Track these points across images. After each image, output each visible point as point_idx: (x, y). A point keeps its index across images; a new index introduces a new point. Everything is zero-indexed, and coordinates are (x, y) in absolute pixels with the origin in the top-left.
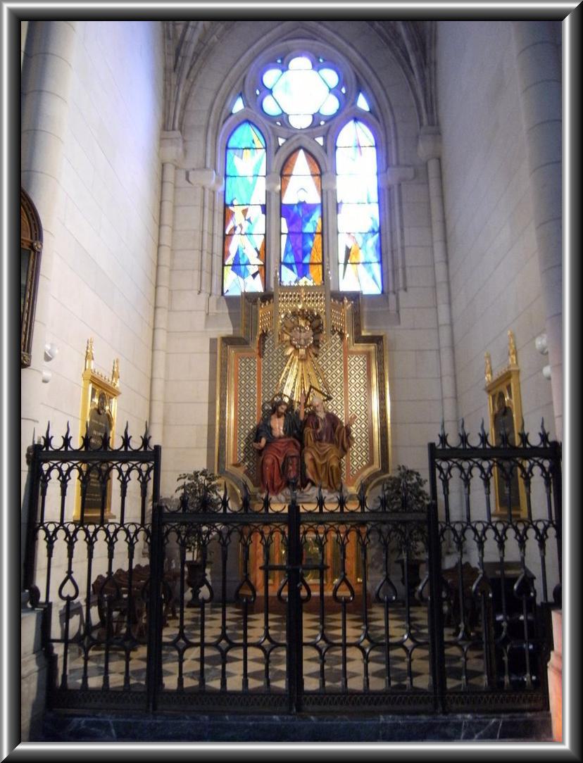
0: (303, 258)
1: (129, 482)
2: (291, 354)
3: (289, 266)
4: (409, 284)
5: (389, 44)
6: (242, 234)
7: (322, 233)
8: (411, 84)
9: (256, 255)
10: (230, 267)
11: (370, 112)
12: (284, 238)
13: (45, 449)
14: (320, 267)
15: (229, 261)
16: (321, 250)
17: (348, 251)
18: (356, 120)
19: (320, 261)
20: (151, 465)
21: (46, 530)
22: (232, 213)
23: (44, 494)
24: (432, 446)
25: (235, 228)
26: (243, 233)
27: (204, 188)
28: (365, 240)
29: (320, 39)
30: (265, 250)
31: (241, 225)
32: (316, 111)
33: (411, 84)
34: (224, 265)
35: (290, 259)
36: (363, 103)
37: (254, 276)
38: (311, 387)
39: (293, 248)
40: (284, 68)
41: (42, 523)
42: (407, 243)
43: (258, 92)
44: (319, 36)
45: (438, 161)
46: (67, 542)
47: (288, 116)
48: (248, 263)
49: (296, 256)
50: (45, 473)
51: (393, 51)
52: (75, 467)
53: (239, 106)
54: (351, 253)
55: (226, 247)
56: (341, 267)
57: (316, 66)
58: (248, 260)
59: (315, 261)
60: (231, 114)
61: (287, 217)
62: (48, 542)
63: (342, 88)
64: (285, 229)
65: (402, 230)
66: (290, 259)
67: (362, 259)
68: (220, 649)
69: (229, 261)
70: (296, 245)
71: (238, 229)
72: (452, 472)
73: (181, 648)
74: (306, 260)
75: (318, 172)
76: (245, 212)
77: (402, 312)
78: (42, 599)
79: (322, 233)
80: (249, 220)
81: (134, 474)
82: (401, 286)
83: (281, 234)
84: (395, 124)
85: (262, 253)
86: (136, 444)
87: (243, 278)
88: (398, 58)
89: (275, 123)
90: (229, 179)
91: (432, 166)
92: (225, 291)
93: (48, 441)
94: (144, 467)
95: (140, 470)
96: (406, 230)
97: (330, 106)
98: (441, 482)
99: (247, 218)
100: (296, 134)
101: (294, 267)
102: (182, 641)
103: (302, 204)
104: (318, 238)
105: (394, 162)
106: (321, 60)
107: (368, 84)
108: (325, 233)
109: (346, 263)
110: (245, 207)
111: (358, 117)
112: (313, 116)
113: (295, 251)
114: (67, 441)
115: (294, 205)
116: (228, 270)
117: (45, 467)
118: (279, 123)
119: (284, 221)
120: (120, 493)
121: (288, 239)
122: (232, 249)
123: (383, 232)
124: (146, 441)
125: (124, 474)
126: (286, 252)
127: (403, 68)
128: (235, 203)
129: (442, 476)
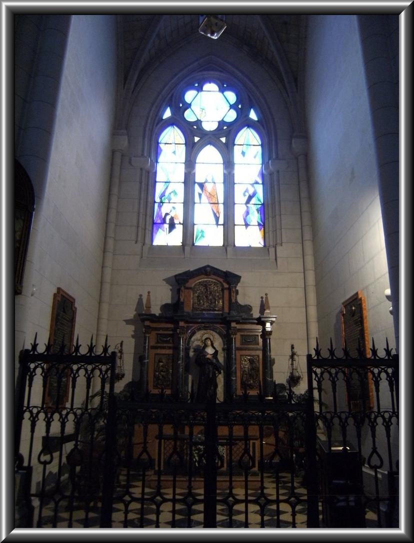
1: (329, 378)
13: (32, 353)
18: (249, 126)
20: (108, 367)
21: (31, 412)
23: (30, 386)
24: (309, 357)
27: (141, 169)
32: (220, 119)
36: (253, 115)
40: (200, 89)
41: (28, 407)
46: (60, 422)
50: (32, 370)
52: (83, 367)
53: (168, 114)
57: (222, 90)
60: (163, 119)
62: (31, 421)
68: (259, 504)
72: (353, 376)
73: (231, 503)
77: (278, 260)
78: (26, 464)
81: (97, 372)
86: (99, 351)
93: (35, 346)
94: (104, 368)
95: (101, 370)
97: (232, 116)
98: (316, 383)
102: (231, 499)
111: (250, 124)
112: (219, 122)
114: (91, 349)
117: (32, 366)
120: (85, 386)
124: (105, 349)
125: (104, 373)
129: (317, 379)
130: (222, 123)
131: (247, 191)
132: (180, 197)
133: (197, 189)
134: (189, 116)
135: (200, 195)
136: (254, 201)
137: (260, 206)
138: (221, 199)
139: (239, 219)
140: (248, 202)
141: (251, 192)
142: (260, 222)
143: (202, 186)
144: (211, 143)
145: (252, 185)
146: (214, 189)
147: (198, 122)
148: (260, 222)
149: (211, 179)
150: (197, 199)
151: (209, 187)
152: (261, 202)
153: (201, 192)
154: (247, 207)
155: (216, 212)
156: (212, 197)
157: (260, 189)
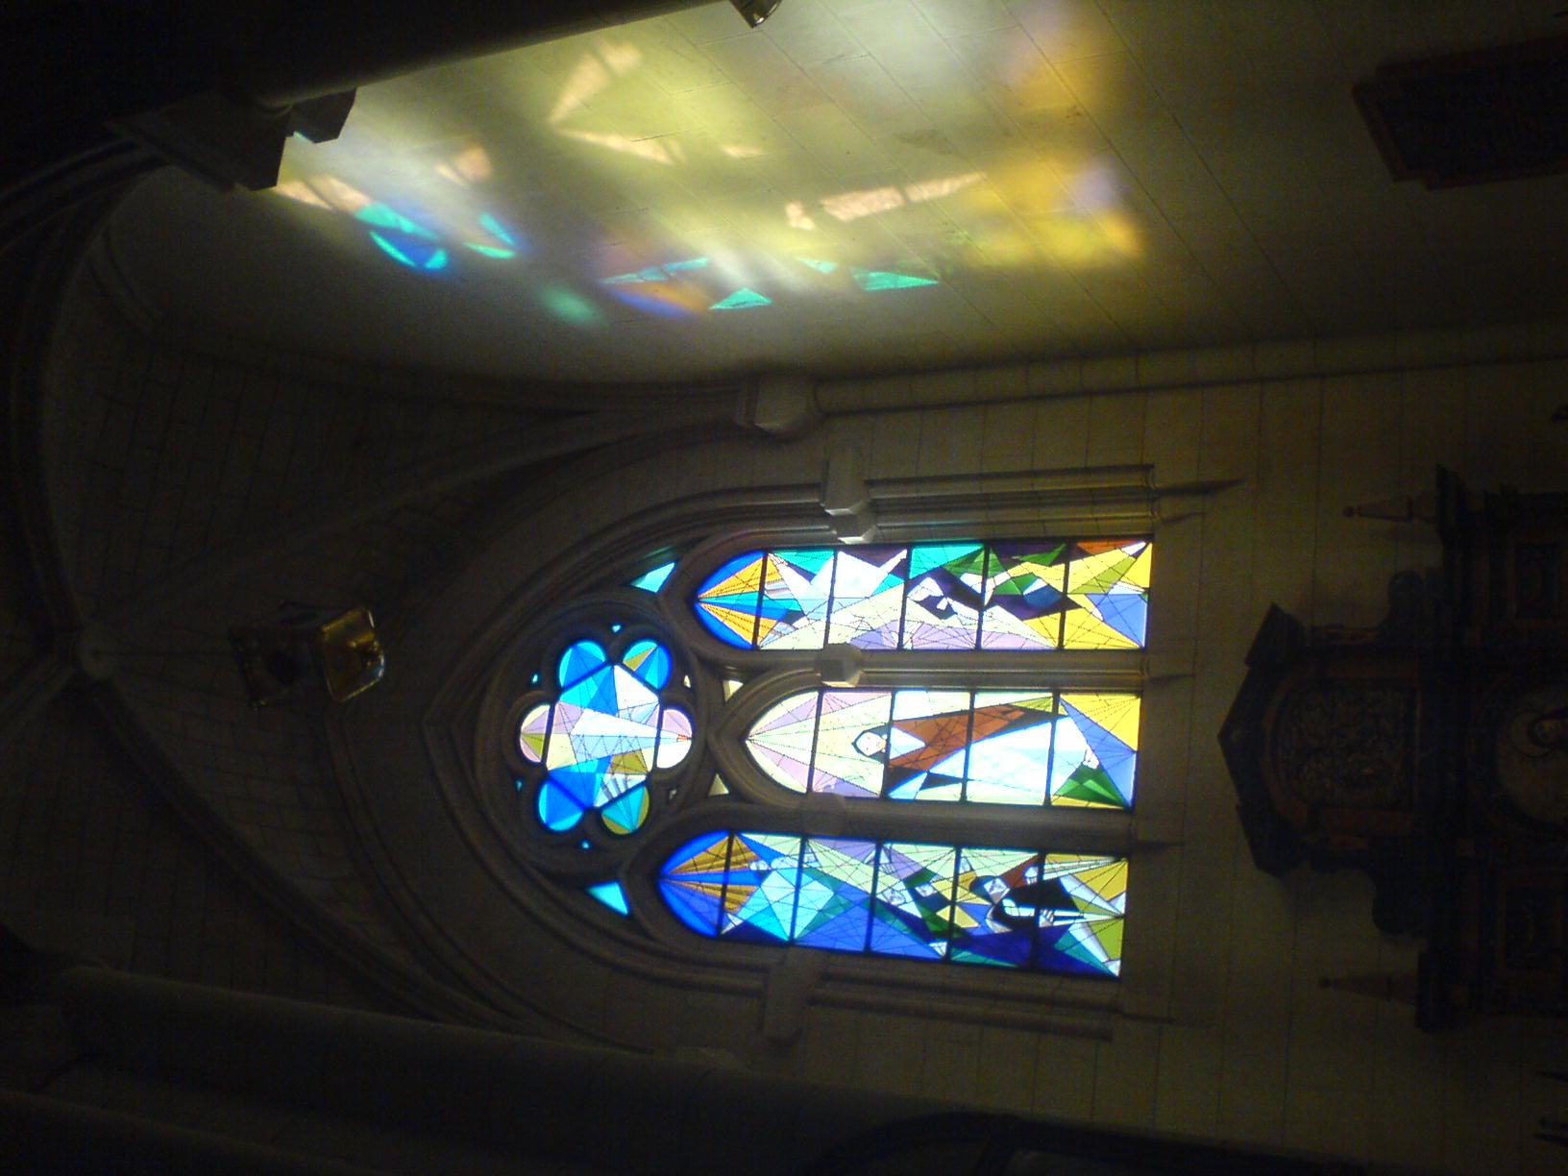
18: (692, 599)
27: (813, 1001)
53: (612, 896)
111: (687, 590)
112: (665, 703)
130: (669, 696)
131: (930, 604)
132: (936, 858)
133: (910, 790)
134: (627, 818)
135: (933, 781)
136: (971, 580)
137: (992, 556)
138: (956, 701)
139: (1037, 633)
140: (973, 599)
141: (931, 587)
142: (1054, 555)
143: (897, 772)
144: (744, 734)
145: (910, 585)
146: (912, 726)
147: (657, 782)
148: (1054, 555)
149: (875, 737)
150: (949, 793)
151: (904, 744)
152: (975, 554)
153: (922, 778)
154: (992, 603)
155: (1003, 723)
156: (945, 735)
157: (928, 557)
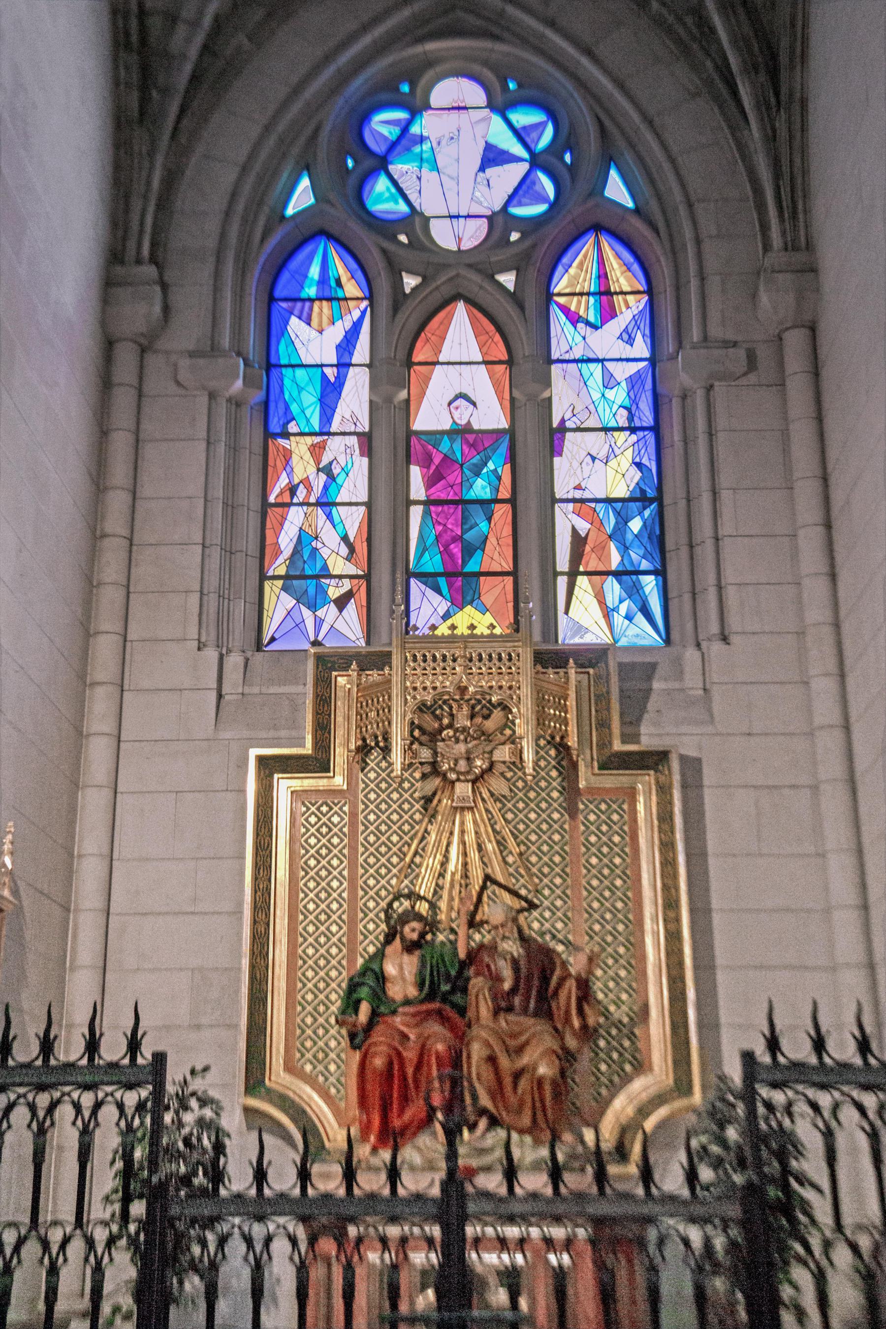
0: (465, 563)
2: (434, 794)
3: (427, 578)
4: (734, 622)
5: (686, 51)
6: (309, 504)
7: (512, 501)
8: (741, 147)
9: (344, 550)
10: (280, 583)
11: (637, 211)
12: (416, 514)
14: (509, 580)
15: (279, 567)
16: (510, 541)
17: (578, 542)
19: (508, 566)
22: (287, 456)
25: (292, 490)
26: (312, 500)
28: (623, 520)
29: (506, 35)
30: (369, 540)
31: (306, 482)
33: (741, 147)
34: (263, 577)
35: (433, 563)
37: (341, 603)
38: (487, 878)
39: (438, 537)
42: (726, 529)
43: (350, 163)
44: (508, 29)
45: (807, 332)
47: (426, 220)
48: (325, 573)
49: (446, 552)
51: (696, 67)
54: (588, 548)
55: (269, 533)
56: (562, 583)
58: (325, 567)
59: (496, 568)
60: (283, 217)
61: (426, 462)
63: (565, 152)
64: (418, 489)
65: (715, 493)
66: (433, 563)
67: (615, 560)
69: (279, 567)
70: (446, 529)
71: (301, 493)
74: (472, 566)
75: (504, 356)
76: (317, 451)
77: (716, 694)
79: (512, 501)
80: (328, 471)
82: (715, 628)
83: (409, 503)
84: (698, 241)
85: (362, 549)
87: (313, 607)
88: (709, 83)
89: (394, 239)
90: (274, 372)
91: (795, 340)
92: (266, 638)
96: (726, 496)
99: (324, 462)
100: (446, 266)
101: (442, 582)
103: (462, 432)
104: (502, 512)
105: (696, 334)
106: (512, 86)
107: (632, 146)
108: (521, 499)
109: (573, 575)
110: (318, 439)
112: (491, 219)
113: (445, 541)
115: (443, 433)
116: (272, 589)
118: (403, 238)
119: (415, 472)
121: (426, 514)
122: (286, 540)
123: (667, 500)
126: (423, 549)
127: (721, 107)
128: (292, 428)
